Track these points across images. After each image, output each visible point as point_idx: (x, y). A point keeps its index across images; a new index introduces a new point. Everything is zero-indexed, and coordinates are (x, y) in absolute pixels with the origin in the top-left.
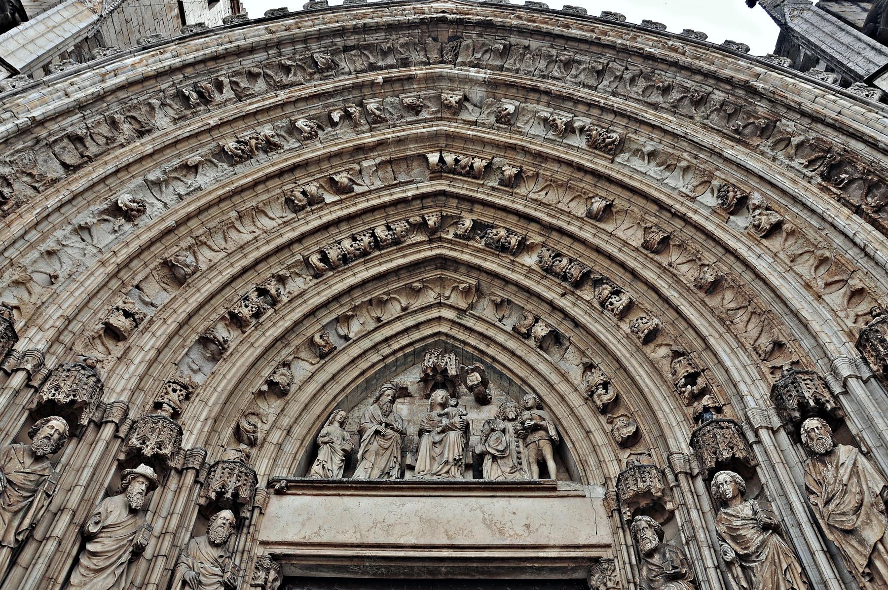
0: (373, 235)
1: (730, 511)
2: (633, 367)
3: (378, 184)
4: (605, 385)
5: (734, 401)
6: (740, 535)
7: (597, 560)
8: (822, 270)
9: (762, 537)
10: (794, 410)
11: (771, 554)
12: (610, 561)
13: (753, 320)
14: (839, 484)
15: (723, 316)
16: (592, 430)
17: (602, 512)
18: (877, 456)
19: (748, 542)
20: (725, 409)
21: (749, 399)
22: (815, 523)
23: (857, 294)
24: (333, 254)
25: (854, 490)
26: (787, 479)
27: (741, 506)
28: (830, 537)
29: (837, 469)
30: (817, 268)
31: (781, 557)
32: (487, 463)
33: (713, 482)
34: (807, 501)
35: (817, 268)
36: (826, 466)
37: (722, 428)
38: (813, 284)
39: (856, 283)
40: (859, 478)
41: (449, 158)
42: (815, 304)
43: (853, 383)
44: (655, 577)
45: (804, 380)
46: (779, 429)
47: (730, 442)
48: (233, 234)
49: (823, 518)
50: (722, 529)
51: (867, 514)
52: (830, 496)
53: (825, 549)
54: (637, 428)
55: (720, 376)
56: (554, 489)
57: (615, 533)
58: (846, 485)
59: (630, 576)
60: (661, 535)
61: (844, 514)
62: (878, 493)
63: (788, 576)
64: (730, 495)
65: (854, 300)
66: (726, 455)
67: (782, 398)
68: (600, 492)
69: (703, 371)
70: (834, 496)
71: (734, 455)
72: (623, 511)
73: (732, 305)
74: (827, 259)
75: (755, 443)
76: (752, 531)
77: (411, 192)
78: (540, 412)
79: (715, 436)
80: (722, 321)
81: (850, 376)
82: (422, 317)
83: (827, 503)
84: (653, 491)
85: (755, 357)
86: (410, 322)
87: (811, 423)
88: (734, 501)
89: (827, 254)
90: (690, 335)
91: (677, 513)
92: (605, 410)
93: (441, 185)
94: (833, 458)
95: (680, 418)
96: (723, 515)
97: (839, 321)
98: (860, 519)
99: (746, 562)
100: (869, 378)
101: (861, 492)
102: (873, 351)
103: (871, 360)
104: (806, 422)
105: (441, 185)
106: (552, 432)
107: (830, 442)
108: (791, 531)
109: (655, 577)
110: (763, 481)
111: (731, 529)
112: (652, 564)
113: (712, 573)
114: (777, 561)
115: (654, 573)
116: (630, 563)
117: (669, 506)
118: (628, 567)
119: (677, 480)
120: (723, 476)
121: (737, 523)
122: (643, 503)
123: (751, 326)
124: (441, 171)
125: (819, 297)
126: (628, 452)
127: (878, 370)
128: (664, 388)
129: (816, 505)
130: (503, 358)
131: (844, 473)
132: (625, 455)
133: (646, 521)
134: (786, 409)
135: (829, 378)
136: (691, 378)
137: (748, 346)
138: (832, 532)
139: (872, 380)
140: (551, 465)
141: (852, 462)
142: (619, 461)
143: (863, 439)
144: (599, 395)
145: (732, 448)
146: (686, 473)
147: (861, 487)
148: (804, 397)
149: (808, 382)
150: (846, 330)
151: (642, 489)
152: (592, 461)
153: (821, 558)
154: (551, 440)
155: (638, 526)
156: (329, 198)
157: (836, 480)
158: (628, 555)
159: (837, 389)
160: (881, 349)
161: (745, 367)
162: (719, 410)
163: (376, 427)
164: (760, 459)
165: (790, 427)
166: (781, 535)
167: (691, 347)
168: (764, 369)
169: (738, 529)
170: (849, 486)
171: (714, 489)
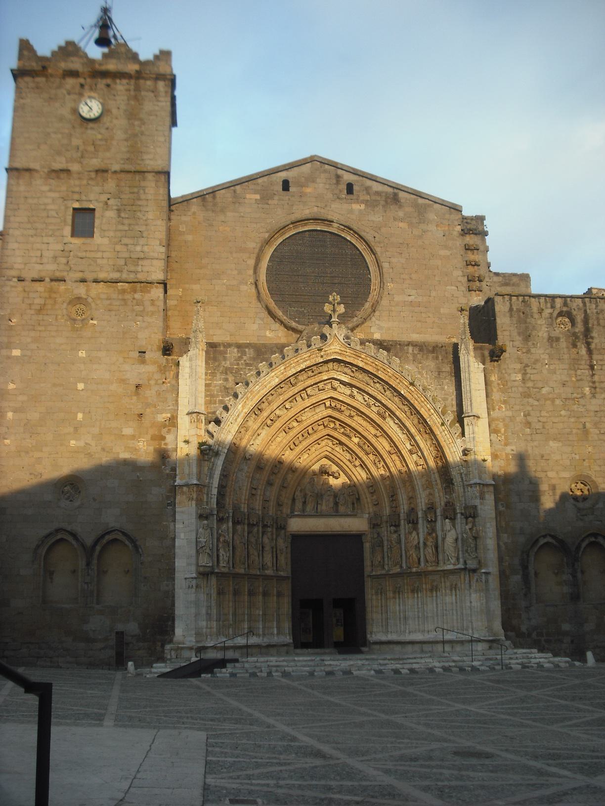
0: (308, 433)
3: (310, 414)
4: (372, 486)
17: (367, 522)
24: (297, 443)
32: (340, 506)
41: (333, 405)
48: (271, 447)
56: (356, 515)
68: (367, 515)
77: (320, 416)
82: (321, 451)
86: (317, 453)
92: (371, 493)
93: (330, 412)
105: (330, 412)
106: (357, 497)
120: (393, 528)
124: (331, 407)
130: (344, 466)
136: (392, 496)
140: (356, 505)
152: (366, 505)
156: (295, 424)
163: (310, 494)
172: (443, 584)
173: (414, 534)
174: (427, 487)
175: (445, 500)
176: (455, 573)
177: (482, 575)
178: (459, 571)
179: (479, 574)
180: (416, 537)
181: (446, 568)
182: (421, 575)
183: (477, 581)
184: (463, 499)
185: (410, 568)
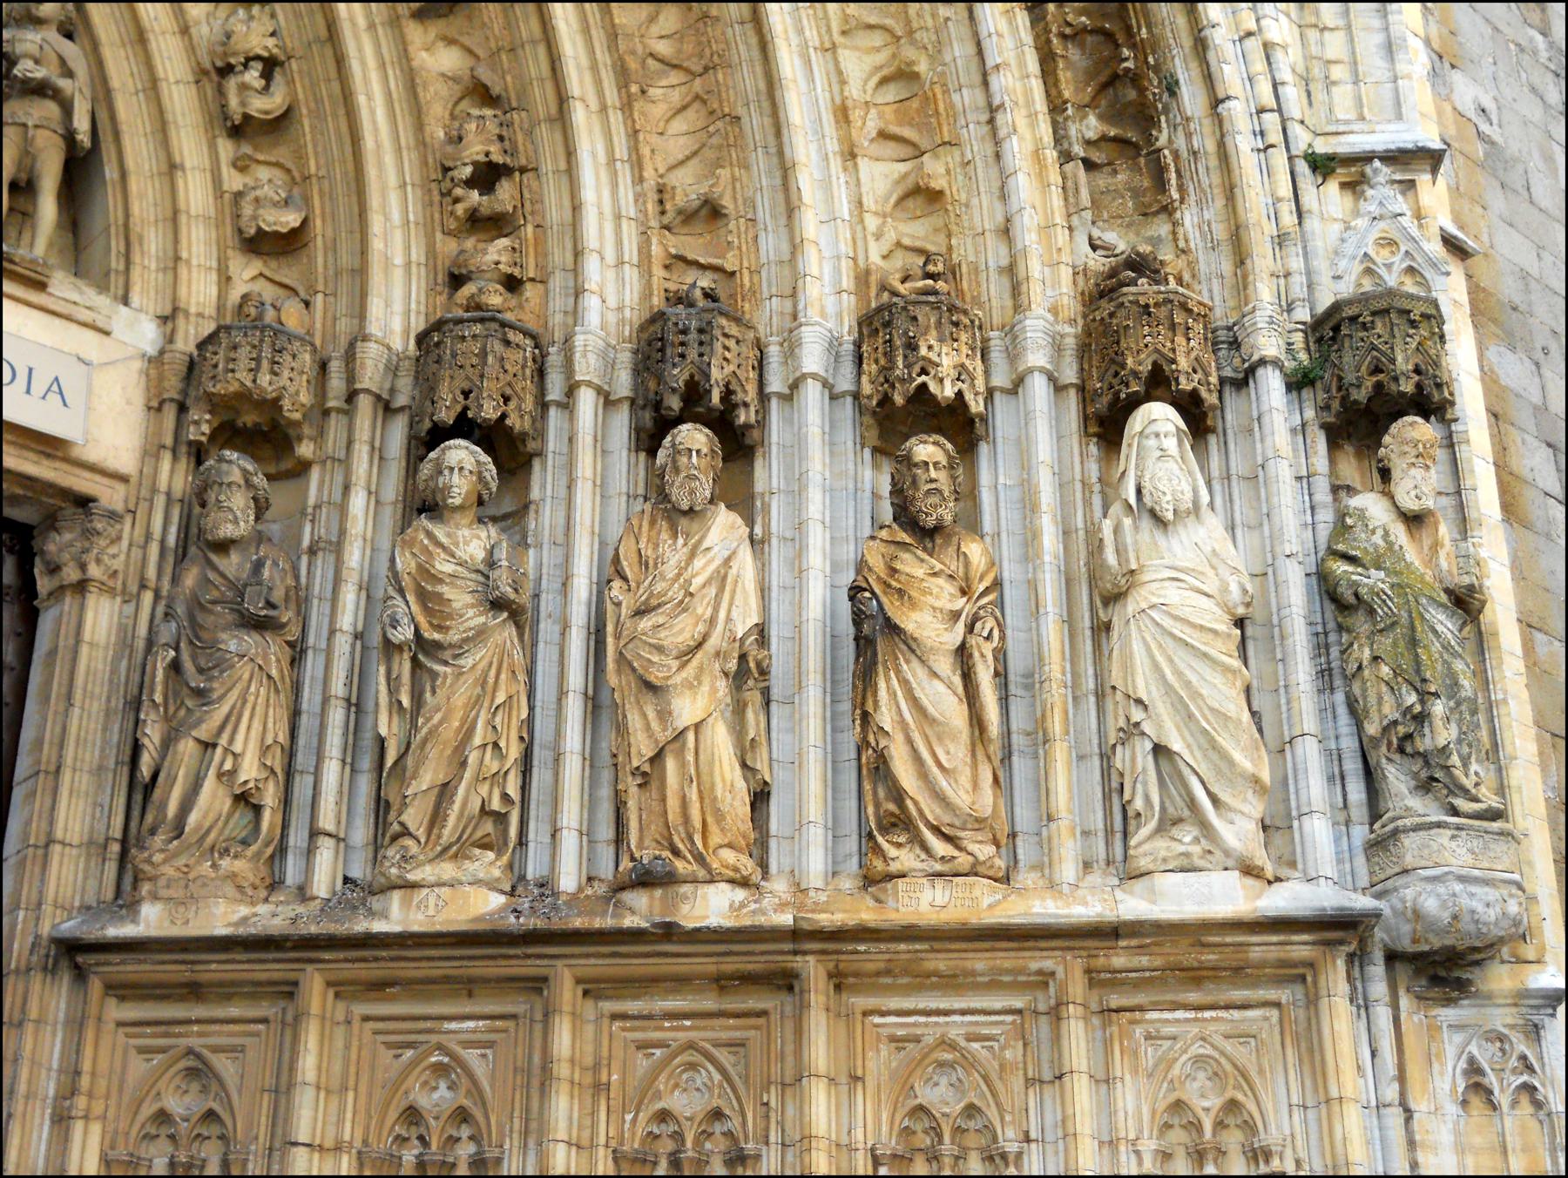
1: (440, 532)
2: (363, 63)
4: (270, 66)
5: (558, 281)
6: (439, 596)
7: (84, 502)
8: (891, 93)
9: (482, 619)
10: (674, 390)
11: (484, 663)
12: (113, 516)
13: (691, 114)
14: (682, 587)
15: (633, 65)
16: (188, 165)
18: (774, 556)
19: (450, 616)
20: (530, 291)
21: (592, 303)
22: (597, 635)
23: (923, 196)
25: (700, 611)
26: (588, 522)
27: (466, 532)
28: (612, 678)
29: (692, 555)
30: (884, 81)
31: (503, 676)
33: (432, 455)
34: (602, 585)
35: (884, 81)
36: (675, 536)
37: (507, 343)
38: (856, 115)
39: (936, 170)
40: (721, 589)
42: (836, 164)
43: (812, 391)
44: (214, 602)
45: (726, 336)
46: (620, 400)
47: (509, 384)
49: (617, 637)
50: (406, 563)
51: (701, 669)
52: (654, 602)
53: (590, 692)
54: (305, 222)
55: (555, 209)
56: (41, 286)
57: (151, 452)
58: (691, 595)
59: (151, 573)
60: (261, 507)
61: (660, 649)
62: (739, 635)
63: (498, 720)
64: (457, 501)
65: (910, 203)
66: (489, 411)
67: (662, 350)
69: (523, 170)
70: (659, 606)
71: (504, 416)
72: (194, 415)
73: (663, 48)
74: (915, 76)
75: (559, 404)
76: (469, 599)
78: (70, 49)
79: (483, 354)
80: (623, 76)
81: (814, 376)
83: (640, 613)
84: (286, 404)
85: (651, 207)
87: (694, 437)
88: (457, 516)
89: (922, 67)
90: (536, 65)
91: (315, 474)
92: (240, 129)
94: (695, 526)
95: (418, 254)
96: (422, 536)
97: (859, 235)
98: (684, 674)
99: (427, 654)
100: (843, 394)
101: (712, 621)
102: (885, 354)
103: (870, 367)
104: (685, 427)
106: (81, 124)
107: (708, 494)
108: (542, 626)
109: (214, 602)
110: (535, 494)
111: (426, 572)
112: (215, 568)
113: (343, 644)
114: (491, 680)
115: (216, 594)
116: (163, 542)
117: (305, 450)
118: (154, 549)
119: (351, 396)
120: (461, 454)
121: (444, 566)
122: (249, 419)
123: (678, 125)
125: (850, 155)
126: (256, 266)
127: (869, 397)
128: (410, 159)
129: (618, 604)
131: (702, 570)
132: (246, 273)
133: (245, 472)
134: (660, 379)
135: (774, 351)
136: (488, 176)
137: (649, 173)
138: (619, 672)
139: (849, 400)
141: (726, 554)
142: (225, 280)
143: (766, 509)
144: (244, 87)
145: (507, 399)
146: (378, 397)
147: (716, 610)
148: (707, 377)
149: (731, 343)
150: (861, 263)
151: (263, 390)
153: (574, 708)
154: (70, 137)
155: (219, 472)
157: (679, 575)
158: (162, 524)
159: (775, 384)
160: (900, 364)
161: (618, 217)
162: (512, 284)
164: (551, 446)
165: (647, 417)
166: (519, 627)
167: (523, 93)
168: (656, 249)
169: (441, 581)
170: (696, 599)
171: (426, 469)
172: (1082, 1092)
173: (723, 527)
174: (883, 135)
175: (1097, 262)
176: (1239, 972)
177: (1534, 1032)
178: (1301, 948)
179: (1501, 1018)
180: (745, 562)
181: (1132, 905)
182: (787, 981)
183: (1477, 1087)
184: (1296, 264)
185: (645, 879)
